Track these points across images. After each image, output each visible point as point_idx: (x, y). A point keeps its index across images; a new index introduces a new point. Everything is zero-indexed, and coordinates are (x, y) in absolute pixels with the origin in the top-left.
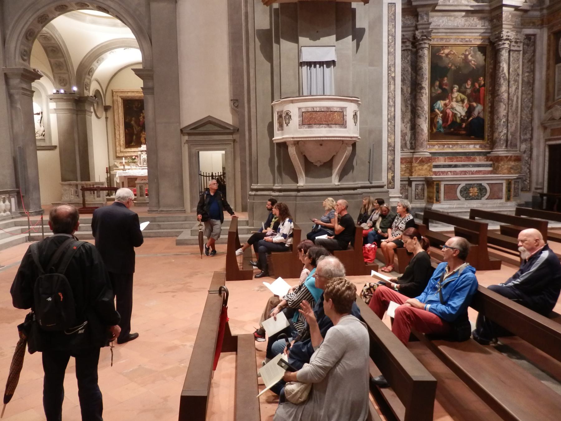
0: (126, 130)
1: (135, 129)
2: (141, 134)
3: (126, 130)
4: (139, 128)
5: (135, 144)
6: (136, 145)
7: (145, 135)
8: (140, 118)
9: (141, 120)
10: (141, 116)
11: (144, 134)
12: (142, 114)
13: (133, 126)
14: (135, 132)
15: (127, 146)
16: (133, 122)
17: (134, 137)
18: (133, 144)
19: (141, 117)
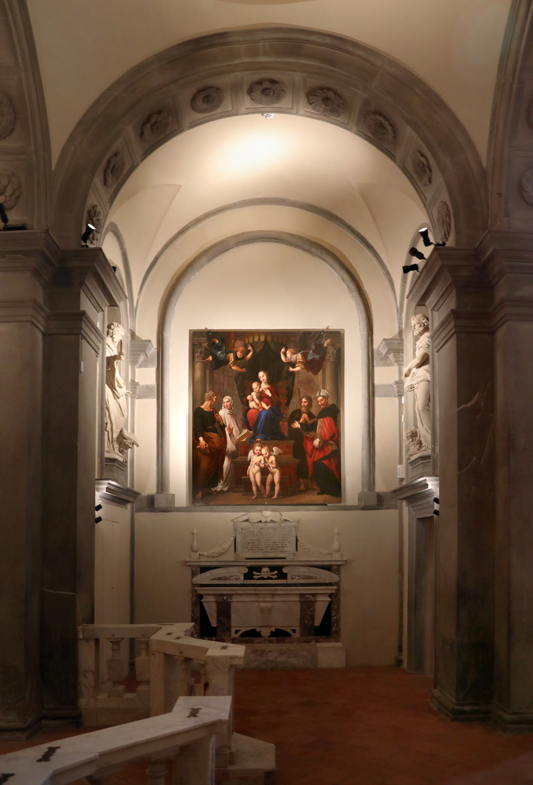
0: (201, 439)
1: (231, 434)
2: (251, 453)
3: (201, 439)
4: (245, 431)
5: (226, 489)
6: (228, 491)
7: (261, 458)
8: (249, 397)
9: (252, 404)
10: (252, 390)
11: (261, 454)
12: (255, 385)
13: (224, 426)
14: (230, 446)
15: (199, 495)
16: (224, 413)
17: (226, 463)
18: (219, 487)
19: (254, 394)
